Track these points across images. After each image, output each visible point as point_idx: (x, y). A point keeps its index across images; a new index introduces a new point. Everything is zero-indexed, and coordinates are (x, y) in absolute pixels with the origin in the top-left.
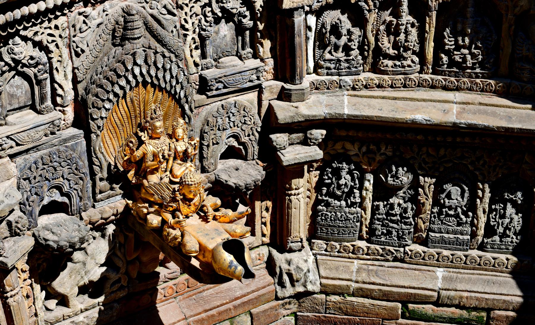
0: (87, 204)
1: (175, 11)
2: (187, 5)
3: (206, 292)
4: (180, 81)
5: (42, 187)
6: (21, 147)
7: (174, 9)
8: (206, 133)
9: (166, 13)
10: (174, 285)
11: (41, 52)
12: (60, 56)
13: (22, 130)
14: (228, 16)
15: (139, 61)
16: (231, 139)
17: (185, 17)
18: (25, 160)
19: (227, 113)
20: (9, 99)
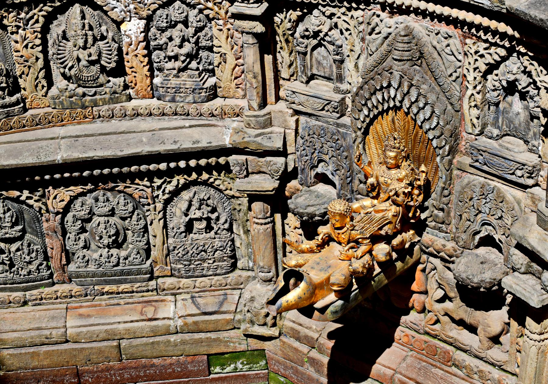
0: (347, 196)
1: (460, 57)
2: (471, 54)
3: (437, 369)
4: (432, 127)
5: (313, 153)
7: (460, 53)
8: (461, 202)
9: (451, 53)
10: (414, 337)
13: (303, 93)
14: (511, 88)
16: (491, 228)
18: (307, 122)
19: (484, 194)
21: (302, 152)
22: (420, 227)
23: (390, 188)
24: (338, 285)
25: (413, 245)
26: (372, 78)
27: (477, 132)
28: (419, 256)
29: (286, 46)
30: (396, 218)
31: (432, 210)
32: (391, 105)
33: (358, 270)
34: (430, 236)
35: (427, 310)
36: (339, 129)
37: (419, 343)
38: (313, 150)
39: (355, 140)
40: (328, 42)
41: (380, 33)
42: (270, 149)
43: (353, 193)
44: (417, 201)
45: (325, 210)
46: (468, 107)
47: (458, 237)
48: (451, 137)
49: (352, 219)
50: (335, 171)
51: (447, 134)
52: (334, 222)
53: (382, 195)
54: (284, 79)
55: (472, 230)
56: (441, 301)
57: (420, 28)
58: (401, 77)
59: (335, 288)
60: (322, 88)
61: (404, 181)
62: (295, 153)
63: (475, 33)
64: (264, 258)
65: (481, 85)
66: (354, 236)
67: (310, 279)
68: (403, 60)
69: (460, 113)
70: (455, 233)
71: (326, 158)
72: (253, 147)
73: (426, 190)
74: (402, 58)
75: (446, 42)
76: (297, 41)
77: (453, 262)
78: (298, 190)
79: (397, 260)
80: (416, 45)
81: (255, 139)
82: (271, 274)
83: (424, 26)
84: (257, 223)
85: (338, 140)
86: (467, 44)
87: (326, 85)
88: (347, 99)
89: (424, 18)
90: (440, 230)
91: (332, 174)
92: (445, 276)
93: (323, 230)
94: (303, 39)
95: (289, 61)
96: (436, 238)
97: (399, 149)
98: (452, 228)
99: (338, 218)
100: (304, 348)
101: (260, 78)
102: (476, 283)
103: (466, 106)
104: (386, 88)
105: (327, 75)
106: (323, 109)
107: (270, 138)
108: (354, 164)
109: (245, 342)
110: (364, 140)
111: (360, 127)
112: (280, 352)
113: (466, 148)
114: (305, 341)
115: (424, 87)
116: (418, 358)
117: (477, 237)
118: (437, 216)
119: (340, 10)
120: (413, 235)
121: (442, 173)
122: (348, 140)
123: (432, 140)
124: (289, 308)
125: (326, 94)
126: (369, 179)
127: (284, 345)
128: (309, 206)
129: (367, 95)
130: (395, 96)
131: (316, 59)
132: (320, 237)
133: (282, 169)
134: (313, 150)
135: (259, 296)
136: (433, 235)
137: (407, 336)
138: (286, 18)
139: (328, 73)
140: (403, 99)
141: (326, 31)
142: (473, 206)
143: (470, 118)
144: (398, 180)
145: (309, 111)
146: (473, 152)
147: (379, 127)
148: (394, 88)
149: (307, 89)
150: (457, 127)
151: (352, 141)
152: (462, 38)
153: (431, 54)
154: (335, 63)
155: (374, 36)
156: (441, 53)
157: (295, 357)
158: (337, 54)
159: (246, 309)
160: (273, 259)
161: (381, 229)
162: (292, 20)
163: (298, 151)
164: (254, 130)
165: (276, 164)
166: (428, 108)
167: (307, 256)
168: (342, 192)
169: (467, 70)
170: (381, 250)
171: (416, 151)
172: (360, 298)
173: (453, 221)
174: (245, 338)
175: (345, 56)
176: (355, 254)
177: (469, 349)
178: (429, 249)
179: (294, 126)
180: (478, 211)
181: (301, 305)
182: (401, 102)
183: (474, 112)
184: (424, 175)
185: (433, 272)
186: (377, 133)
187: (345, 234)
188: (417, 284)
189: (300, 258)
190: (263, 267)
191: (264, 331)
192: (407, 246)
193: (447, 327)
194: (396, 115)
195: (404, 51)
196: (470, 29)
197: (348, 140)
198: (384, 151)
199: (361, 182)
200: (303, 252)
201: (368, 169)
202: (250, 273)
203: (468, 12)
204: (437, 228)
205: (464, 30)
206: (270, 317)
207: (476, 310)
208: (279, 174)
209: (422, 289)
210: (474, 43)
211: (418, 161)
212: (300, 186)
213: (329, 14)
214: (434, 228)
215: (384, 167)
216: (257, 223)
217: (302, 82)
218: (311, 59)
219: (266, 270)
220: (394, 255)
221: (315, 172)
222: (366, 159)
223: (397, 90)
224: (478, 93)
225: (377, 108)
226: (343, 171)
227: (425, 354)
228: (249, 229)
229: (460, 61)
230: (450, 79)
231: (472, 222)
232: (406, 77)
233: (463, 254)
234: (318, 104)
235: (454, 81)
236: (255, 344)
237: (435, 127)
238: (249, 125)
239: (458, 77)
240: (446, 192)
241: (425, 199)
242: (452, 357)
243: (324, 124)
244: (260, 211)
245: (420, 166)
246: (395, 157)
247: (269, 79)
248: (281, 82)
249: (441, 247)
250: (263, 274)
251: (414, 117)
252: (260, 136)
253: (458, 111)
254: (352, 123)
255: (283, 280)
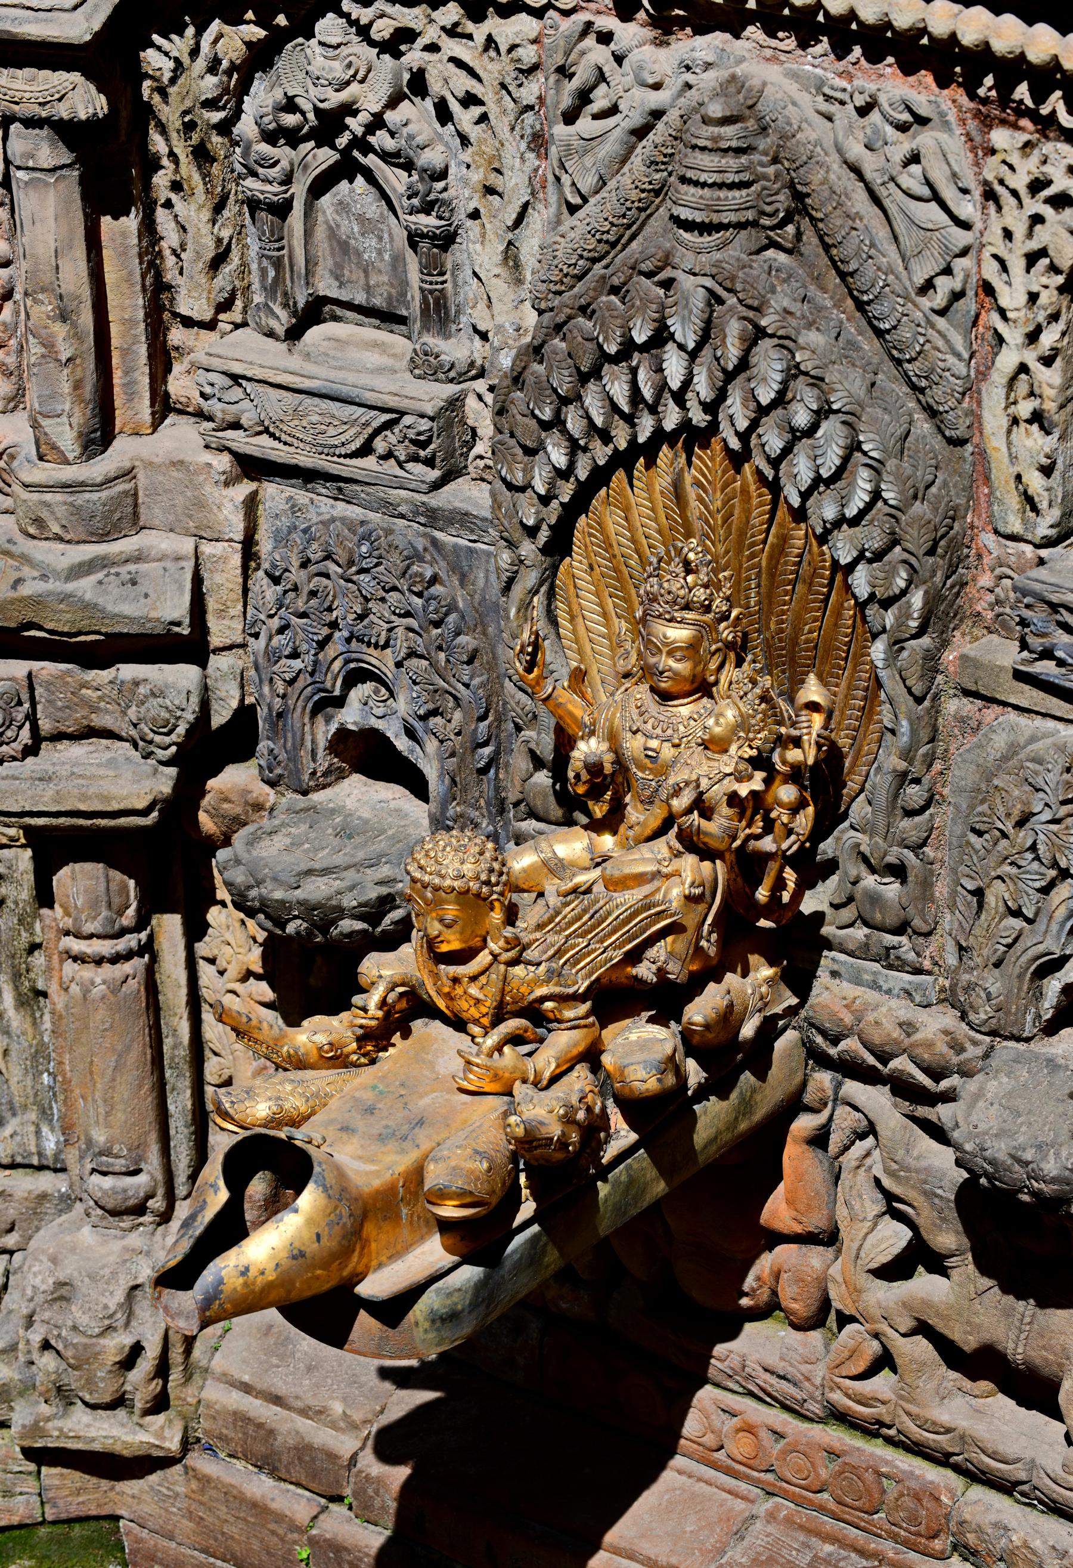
1: (967, 209)
4: (851, 512)
5: (322, 644)
6: (276, 444)
7: (965, 191)
8: (980, 834)
9: (926, 192)
10: (779, 1435)
11: (443, 125)
12: (498, 171)
15: (675, 325)
17: (1000, 247)
18: (295, 508)
20: (333, 254)
21: (275, 642)
22: (799, 949)
23: (671, 781)
24: (466, 1199)
25: (769, 1030)
26: (583, 310)
27: (1043, 528)
28: (798, 1078)
29: (196, 177)
30: (701, 908)
31: (853, 872)
32: (669, 425)
33: (545, 1132)
34: (847, 989)
35: (832, 1316)
36: (439, 535)
37: (802, 1461)
38: (325, 631)
39: (510, 582)
40: (386, 156)
41: (613, 110)
42: (134, 629)
43: (502, 811)
44: (790, 832)
45: (384, 890)
46: (1005, 422)
47: (969, 988)
48: (931, 552)
49: (511, 915)
50: (424, 718)
51: (916, 539)
52: (435, 928)
53: (634, 813)
54: (188, 322)
55: (1031, 953)
56: (895, 1270)
57: (792, 88)
58: (714, 299)
59: (449, 1211)
60: (359, 357)
61: (733, 749)
62: (243, 646)
63: (1029, 102)
64: (112, 1112)
65: (1061, 326)
66: (524, 989)
67: (340, 1173)
68: (721, 227)
69: (969, 448)
70: (952, 973)
71: (384, 662)
72: (59, 621)
73: (825, 785)
74: (716, 218)
75: (903, 145)
76: (246, 154)
77: (948, 1097)
78: (258, 807)
79: (702, 1093)
80: (775, 160)
81: (70, 587)
82: (142, 1179)
83: (808, 76)
84: (79, 958)
85: (434, 580)
86: (993, 152)
87: (375, 345)
88: (471, 402)
89: (803, 45)
90: (888, 959)
91: (410, 733)
92: (913, 1163)
93: (382, 970)
94: (273, 143)
95: (211, 244)
96: (872, 996)
97: (707, 609)
98: (942, 948)
99: (451, 910)
100: (296, 1503)
101: (86, 319)
102: (1054, 1180)
103: (994, 420)
104: (645, 348)
105: (378, 302)
106: (365, 450)
107: (134, 583)
108: (508, 685)
109: (30, 1485)
110: (549, 581)
111: (531, 522)
112: (188, 1525)
113: (998, 602)
114: (298, 1473)
115: (812, 338)
116: (801, 1527)
117: (1053, 986)
118: (875, 899)
119: (435, 15)
120: (770, 981)
121: (897, 713)
122: (481, 582)
123: (850, 568)
124: (249, 1303)
125: (380, 382)
126: (582, 745)
127: (202, 1491)
128: (310, 872)
129: (563, 383)
130: (687, 383)
131: (332, 233)
132: (373, 999)
133: (191, 717)
134: (325, 631)
135: (92, 1277)
136: (858, 982)
137: (749, 1429)
138: (195, 52)
139: (384, 290)
140: (722, 395)
141: (376, 108)
142: (1033, 848)
143: (1015, 470)
144: (705, 745)
145: (306, 460)
146: (1027, 614)
147: (614, 520)
148: (681, 347)
149: (294, 362)
150: (955, 509)
151: (496, 585)
152: (972, 125)
153: (839, 199)
154: (413, 245)
155: (585, 125)
156: (882, 192)
157: (256, 1545)
158: (427, 208)
159: (36, 1337)
160: (151, 1115)
161: (634, 957)
162: (225, 64)
163: (256, 636)
164: (61, 546)
165: (162, 694)
166: (829, 427)
167: (320, 1079)
168: (454, 809)
169: (995, 265)
170: (640, 1048)
171: (783, 615)
172: (552, 1257)
173: (947, 921)
174: (32, 1467)
175: (460, 216)
176: (530, 1065)
177: (1023, 1476)
178: (843, 1045)
179: (237, 528)
180: (1053, 873)
181: (302, 1290)
182: (711, 408)
183: (1029, 443)
184: (818, 719)
185: (860, 1147)
186: (608, 546)
187: (483, 979)
188: (790, 1202)
189: (289, 1087)
190: (107, 1152)
191: (116, 1432)
192: (748, 1031)
193: (926, 1386)
194: (689, 463)
195: (721, 186)
196: (1005, 88)
197: (481, 582)
198: (643, 621)
199: (538, 763)
200: (300, 1064)
201: (574, 705)
202: (46, 1182)
203: (997, 13)
204: (874, 950)
205: (981, 92)
206: (146, 1364)
207: (1042, 1304)
208: (174, 737)
209: (815, 1222)
210: (1027, 145)
211: (789, 663)
212: (267, 789)
213: (386, 34)
214: (863, 952)
215: (642, 693)
216: (79, 958)
217: (270, 334)
218: (308, 234)
219: (119, 1164)
220: (695, 1073)
221: (333, 728)
222: (560, 660)
223: (693, 356)
224: (1047, 361)
225: (606, 437)
226: (458, 716)
227: (832, 1505)
228: (40, 985)
229: (966, 225)
230: (925, 303)
231: (1030, 921)
232: (732, 301)
233: (994, 1062)
234: (346, 427)
235: (942, 312)
236: (73, 1492)
237: (862, 513)
238: (38, 528)
239: (957, 296)
240: (914, 794)
241: (822, 830)
242: (947, 1516)
243: (371, 515)
244: (94, 905)
245: (797, 682)
246: (692, 647)
247: (124, 322)
248: (177, 335)
249: (897, 1033)
250: (108, 1182)
251: (769, 473)
252: (89, 573)
253: (961, 442)
254: (496, 505)
255: (221, 1183)
